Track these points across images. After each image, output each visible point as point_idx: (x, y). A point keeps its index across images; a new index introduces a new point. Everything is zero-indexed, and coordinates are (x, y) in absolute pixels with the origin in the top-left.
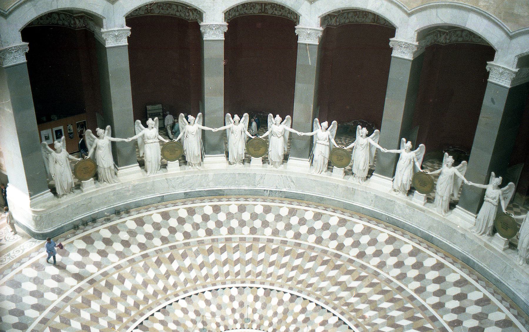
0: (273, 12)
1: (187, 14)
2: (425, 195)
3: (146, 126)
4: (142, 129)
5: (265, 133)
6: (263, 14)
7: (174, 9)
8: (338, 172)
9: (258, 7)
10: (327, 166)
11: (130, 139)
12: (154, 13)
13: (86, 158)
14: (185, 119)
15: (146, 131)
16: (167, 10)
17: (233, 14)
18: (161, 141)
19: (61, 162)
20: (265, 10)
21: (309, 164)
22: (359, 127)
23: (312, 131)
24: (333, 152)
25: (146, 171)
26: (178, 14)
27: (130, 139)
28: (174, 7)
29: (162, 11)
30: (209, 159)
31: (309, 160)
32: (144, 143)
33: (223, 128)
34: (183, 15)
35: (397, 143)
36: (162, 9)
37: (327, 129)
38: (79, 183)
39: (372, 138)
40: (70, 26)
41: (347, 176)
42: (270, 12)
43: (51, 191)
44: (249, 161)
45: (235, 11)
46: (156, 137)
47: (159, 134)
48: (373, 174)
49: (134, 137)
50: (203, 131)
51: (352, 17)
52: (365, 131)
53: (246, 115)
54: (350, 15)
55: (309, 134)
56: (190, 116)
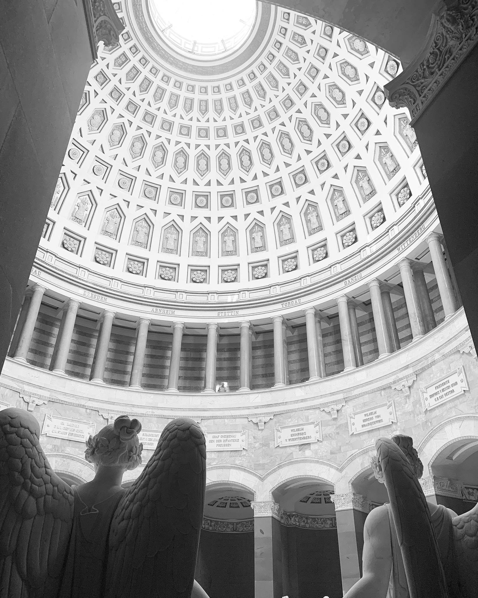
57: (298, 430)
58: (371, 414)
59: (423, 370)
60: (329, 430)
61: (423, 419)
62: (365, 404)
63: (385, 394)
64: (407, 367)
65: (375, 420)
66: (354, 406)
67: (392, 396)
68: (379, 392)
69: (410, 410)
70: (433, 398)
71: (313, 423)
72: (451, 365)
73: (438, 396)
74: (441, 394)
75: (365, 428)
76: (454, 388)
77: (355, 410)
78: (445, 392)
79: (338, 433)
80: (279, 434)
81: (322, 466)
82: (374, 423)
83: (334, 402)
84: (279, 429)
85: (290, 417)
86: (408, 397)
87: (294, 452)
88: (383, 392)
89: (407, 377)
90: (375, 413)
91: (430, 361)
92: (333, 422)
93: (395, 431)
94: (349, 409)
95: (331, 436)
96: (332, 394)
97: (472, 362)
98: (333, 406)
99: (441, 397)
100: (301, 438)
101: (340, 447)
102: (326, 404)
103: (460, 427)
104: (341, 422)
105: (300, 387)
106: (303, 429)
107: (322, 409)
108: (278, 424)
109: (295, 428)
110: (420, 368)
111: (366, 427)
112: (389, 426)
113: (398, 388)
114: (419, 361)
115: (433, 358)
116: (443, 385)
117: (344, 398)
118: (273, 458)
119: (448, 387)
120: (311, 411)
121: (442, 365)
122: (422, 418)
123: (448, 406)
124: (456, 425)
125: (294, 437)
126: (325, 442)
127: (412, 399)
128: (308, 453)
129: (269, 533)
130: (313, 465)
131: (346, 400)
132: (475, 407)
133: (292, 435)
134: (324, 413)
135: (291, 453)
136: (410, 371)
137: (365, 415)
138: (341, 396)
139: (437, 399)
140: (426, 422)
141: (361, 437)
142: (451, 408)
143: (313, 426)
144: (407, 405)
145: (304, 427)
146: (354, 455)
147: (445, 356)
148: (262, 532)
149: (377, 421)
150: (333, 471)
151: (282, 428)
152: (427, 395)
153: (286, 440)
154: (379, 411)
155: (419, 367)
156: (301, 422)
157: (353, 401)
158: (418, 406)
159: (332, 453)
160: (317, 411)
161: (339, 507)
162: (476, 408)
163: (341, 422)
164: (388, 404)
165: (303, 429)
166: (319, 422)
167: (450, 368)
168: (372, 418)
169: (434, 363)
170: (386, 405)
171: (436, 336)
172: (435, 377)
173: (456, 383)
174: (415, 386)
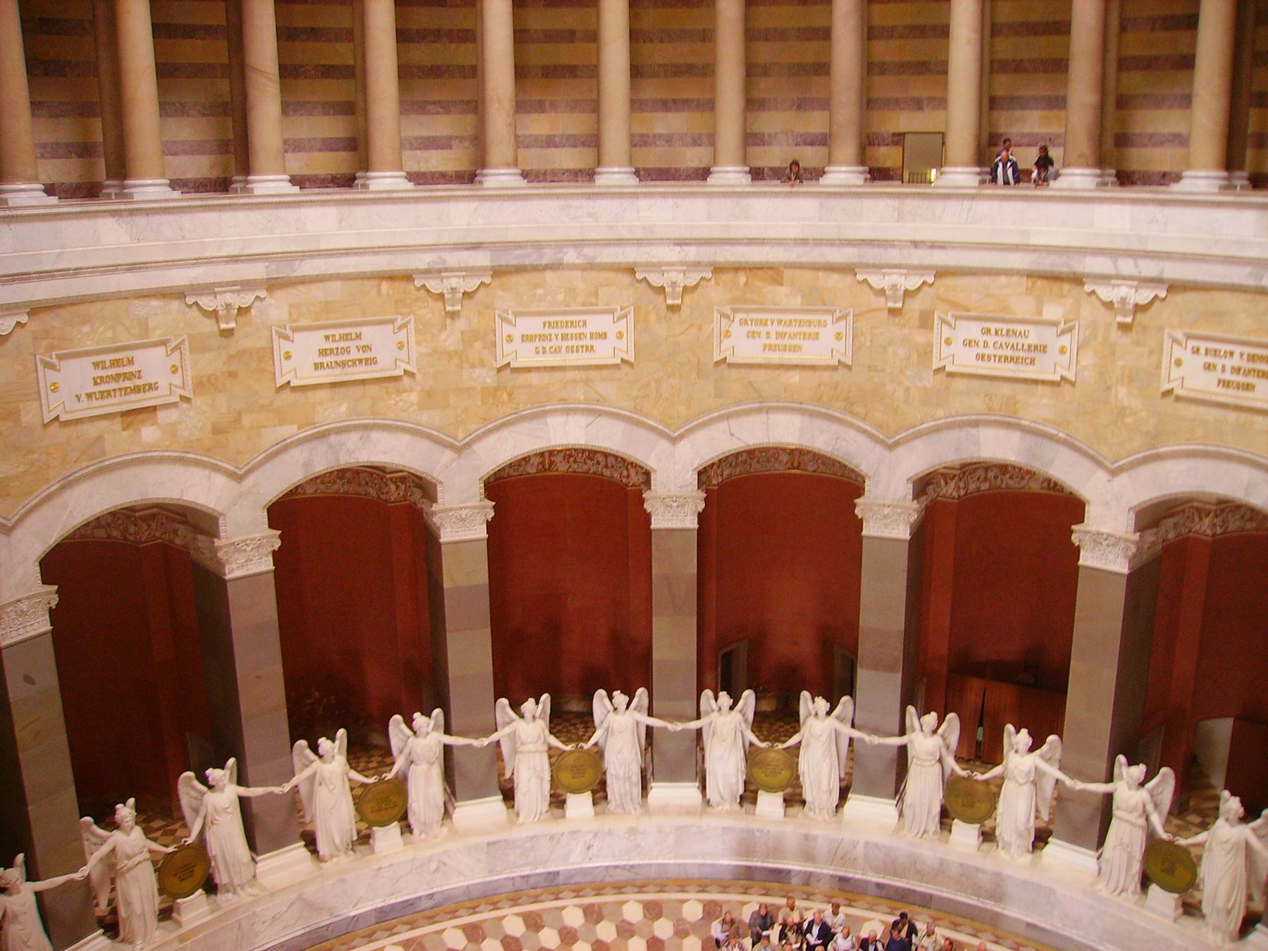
0: (818, 468)
1: (625, 473)
2: (1176, 895)
3: (522, 716)
4: (513, 721)
5: (790, 737)
6: (795, 471)
7: (598, 463)
8: (964, 834)
9: (785, 458)
10: (937, 819)
11: (485, 741)
12: (557, 470)
13: (385, 777)
14: (607, 701)
15: (519, 724)
16: (586, 464)
17: (726, 473)
18: (550, 748)
19: (331, 783)
20: (799, 464)
21: (895, 813)
22: (1010, 727)
23: (902, 731)
24: (951, 785)
25: (518, 815)
26: (607, 473)
27: (485, 741)
28: (602, 459)
29: (575, 466)
30: (661, 792)
31: (896, 802)
32: (515, 752)
33: (694, 725)
34: (616, 475)
35: (1102, 766)
36: (575, 461)
37: (935, 732)
38: (367, 832)
39: (1042, 757)
40: (379, 498)
41: (986, 846)
42: (811, 468)
43: (305, 846)
44: (754, 801)
45: (731, 465)
46: (539, 739)
47: (551, 733)
48: (1050, 839)
49: (494, 737)
50: (649, 730)
51: (996, 478)
52: (1023, 738)
53: (748, 696)
54: (991, 474)
55: (897, 741)
56: (617, 694)
57: (116, 363)
58: (346, 337)
59: (520, 269)
60: (211, 363)
61: (489, 380)
62: (327, 307)
63: (391, 292)
64: (476, 246)
65: (355, 355)
66: (291, 306)
67: (408, 301)
68: (374, 283)
69: (452, 348)
70: (531, 346)
71: (163, 343)
72: (602, 291)
73: (547, 345)
74: (555, 343)
75: (322, 372)
76: (597, 344)
77: (295, 316)
78: (570, 343)
79: (233, 375)
80: (52, 376)
81: (192, 469)
82: (354, 362)
83: (234, 283)
84: (54, 360)
85: (87, 320)
86: (453, 315)
87: (106, 436)
88: (385, 286)
89: (470, 271)
90: (359, 336)
91: (548, 257)
92: (220, 341)
93: (406, 391)
94: (275, 308)
95: (213, 381)
96: (234, 259)
97: (655, 306)
98: (228, 295)
99: (557, 350)
100: (126, 391)
101: (240, 413)
102: (208, 289)
103: (588, 426)
104: (244, 341)
105: (115, 213)
106: (131, 361)
107: (190, 300)
108: (45, 343)
109: (107, 358)
110: (514, 262)
111: (328, 372)
112: (396, 379)
113: (434, 286)
114: (518, 245)
115: (561, 255)
116: (567, 326)
117: (269, 279)
118: (36, 456)
119: (580, 336)
120: (155, 303)
121: (577, 278)
122: (488, 378)
123: (570, 375)
124: (582, 420)
125: (104, 387)
126: (198, 401)
127: (461, 324)
128: (149, 433)
129: (48, 677)
130: (164, 469)
131: (273, 285)
132: (637, 397)
133: (98, 381)
134: (195, 312)
135: (99, 439)
136: (482, 259)
137: (327, 337)
138: (257, 271)
139: (541, 350)
140: (497, 389)
141: (310, 394)
142: (575, 381)
143: (160, 351)
144: (444, 335)
145: (139, 356)
146: (288, 441)
147: (591, 266)
148: (29, 680)
149: (360, 361)
150: (220, 480)
151: (61, 358)
152: (516, 334)
153: (78, 398)
154: (369, 334)
155: (511, 259)
156: (125, 340)
157: (291, 290)
158: (478, 345)
159: (216, 430)
160: (175, 305)
161: (235, 570)
162: (638, 401)
163: (244, 341)
164: (399, 322)
165: (131, 361)
166: (183, 342)
167: (596, 294)
168: (347, 351)
169: (557, 267)
170: (392, 322)
171: (575, 203)
172: (549, 298)
173: (603, 336)
174: (481, 295)
